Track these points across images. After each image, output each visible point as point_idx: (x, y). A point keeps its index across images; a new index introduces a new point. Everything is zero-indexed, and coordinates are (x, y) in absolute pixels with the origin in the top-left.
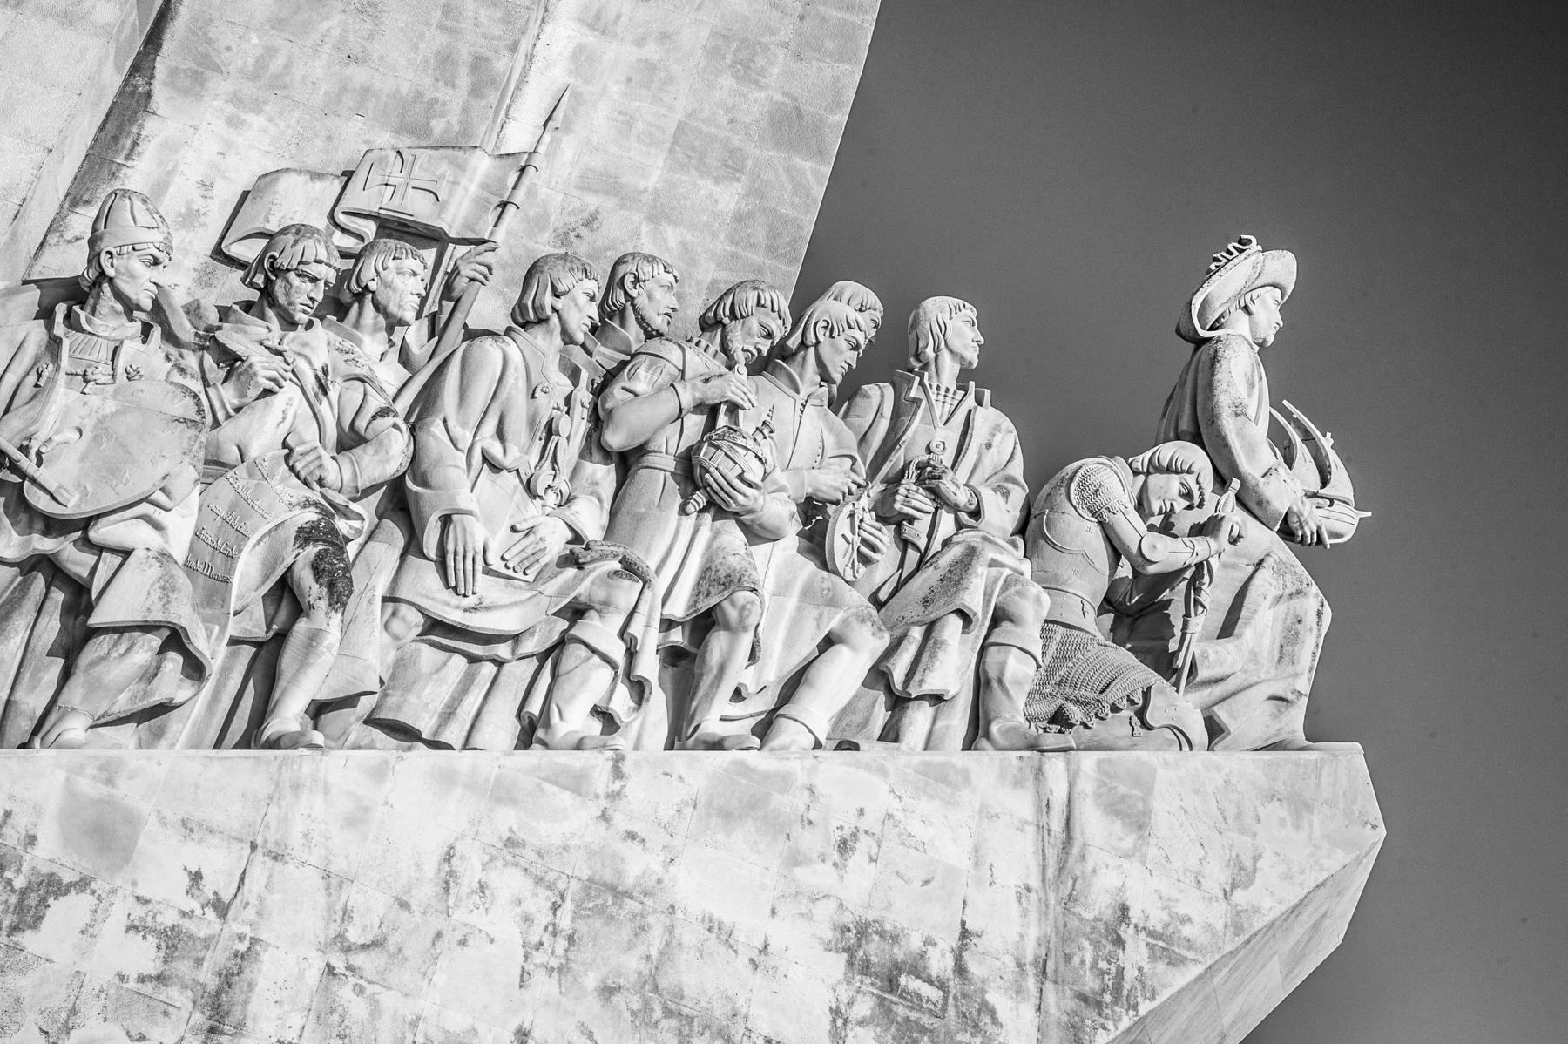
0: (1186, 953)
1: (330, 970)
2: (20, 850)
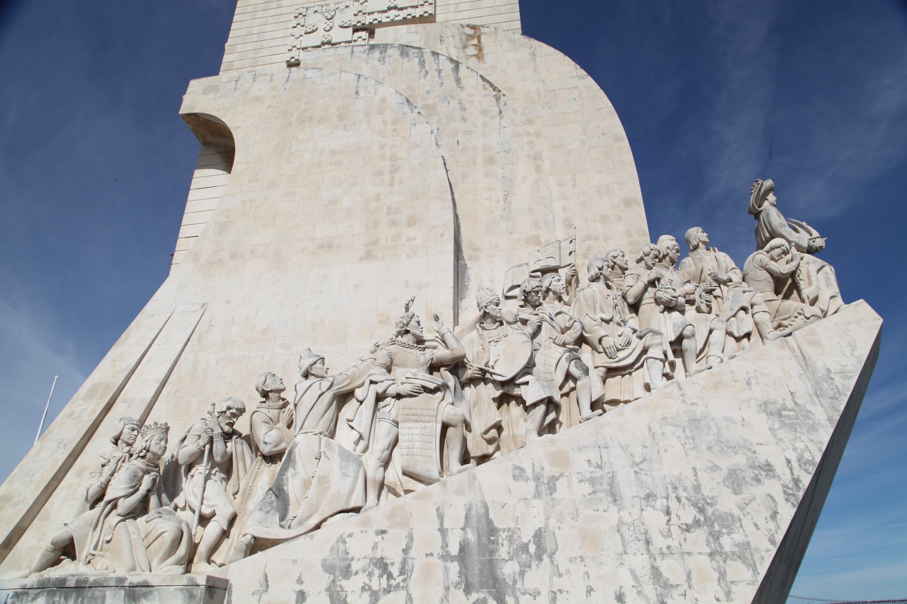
0: (851, 374)
1: (636, 472)
2: (541, 472)
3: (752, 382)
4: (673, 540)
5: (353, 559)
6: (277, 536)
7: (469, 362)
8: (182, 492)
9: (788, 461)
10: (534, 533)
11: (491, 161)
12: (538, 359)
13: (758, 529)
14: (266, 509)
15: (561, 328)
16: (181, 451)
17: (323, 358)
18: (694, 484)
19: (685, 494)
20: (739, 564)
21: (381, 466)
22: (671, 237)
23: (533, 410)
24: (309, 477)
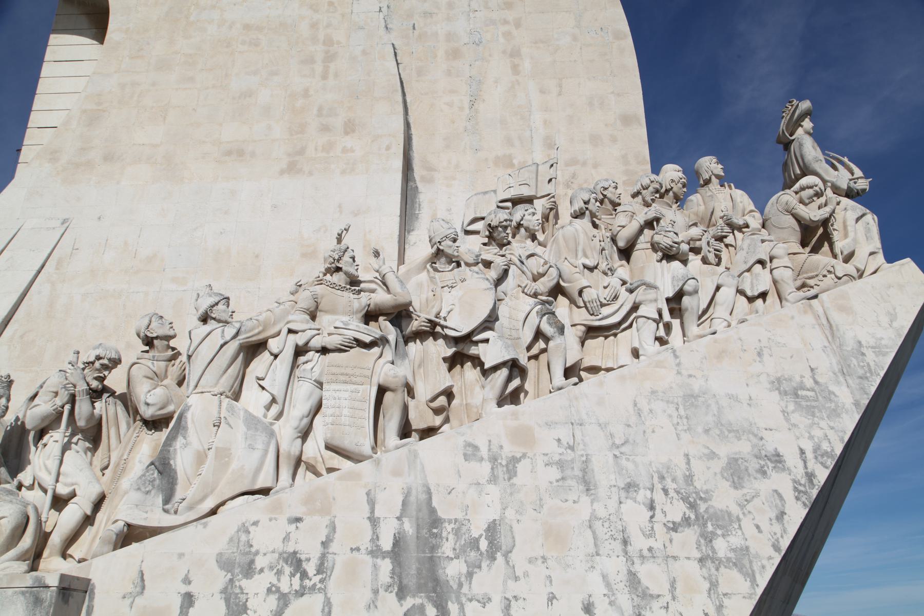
0: (888, 350)
1: (615, 456)
2: (499, 452)
3: (764, 352)
4: (656, 540)
5: (257, 553)
6: (159, 523)
7: (415, 311)
8: (29, 466)
9: (802, 452)
10: (486, 526)
11: (455, 54)
12: (503, 311)
13: (760, 531)
14: (146, 488)
15: (533, 274)
16: (29, 412)
17: (228, 298)
18: (685, 474)
19: (674, 486)
20: (735, 573)
21: (298, 437)
22: (677, 167)
23: (493, 374)
24: (204, 449)
